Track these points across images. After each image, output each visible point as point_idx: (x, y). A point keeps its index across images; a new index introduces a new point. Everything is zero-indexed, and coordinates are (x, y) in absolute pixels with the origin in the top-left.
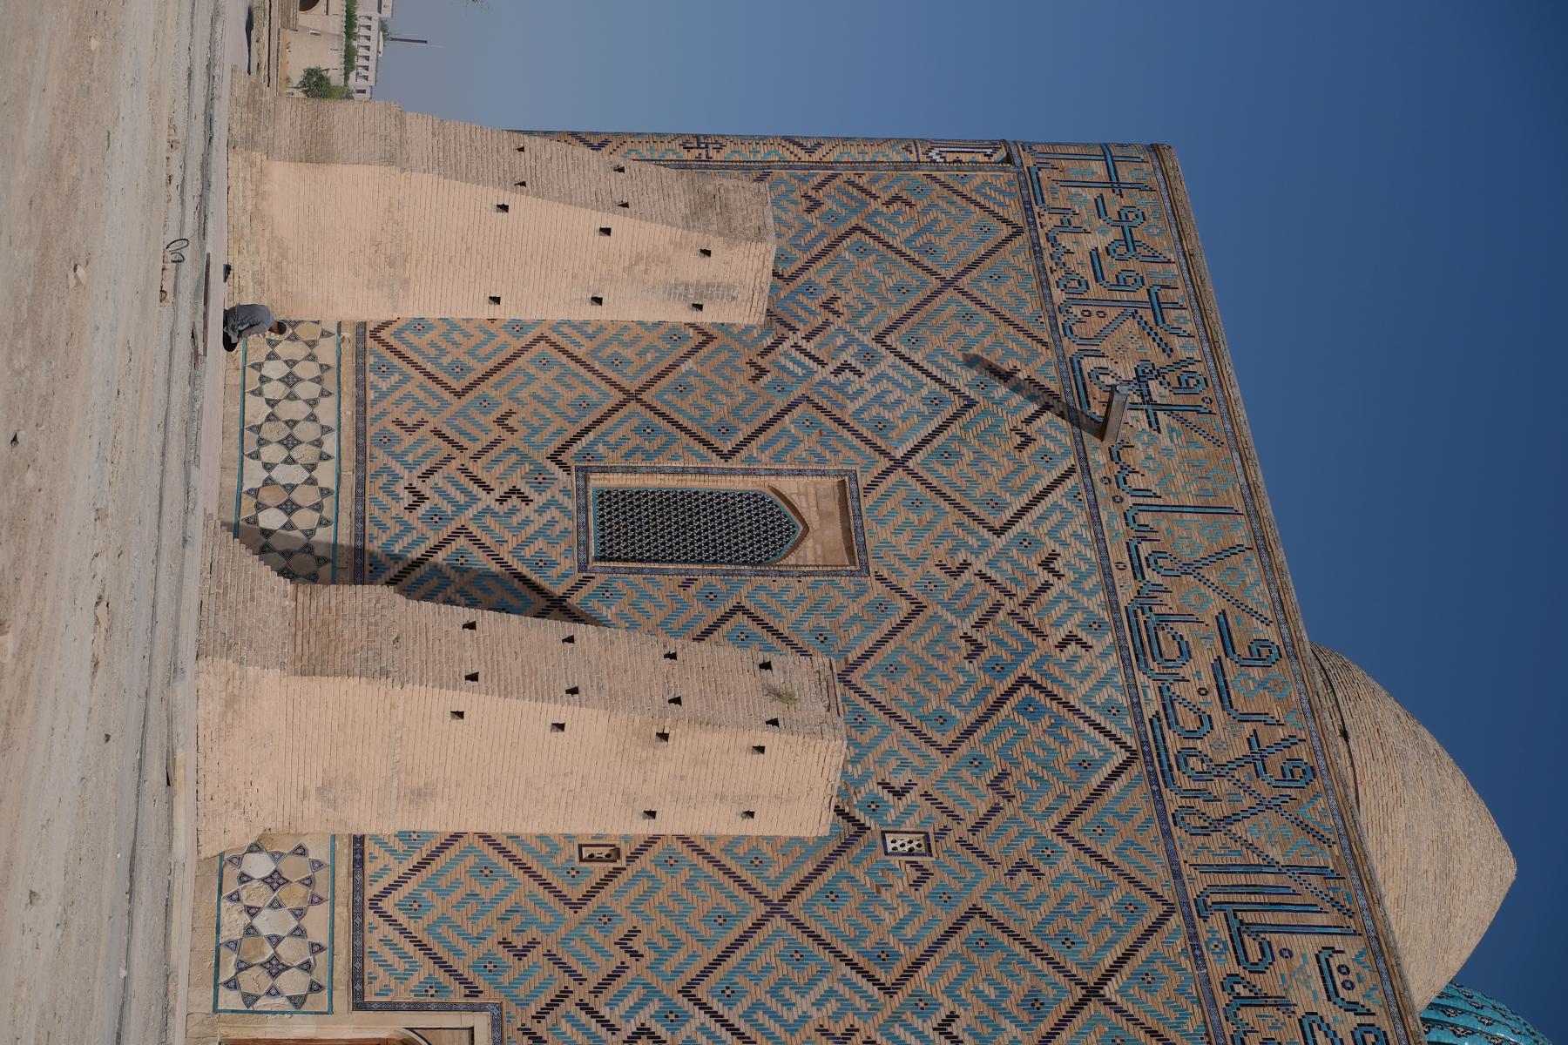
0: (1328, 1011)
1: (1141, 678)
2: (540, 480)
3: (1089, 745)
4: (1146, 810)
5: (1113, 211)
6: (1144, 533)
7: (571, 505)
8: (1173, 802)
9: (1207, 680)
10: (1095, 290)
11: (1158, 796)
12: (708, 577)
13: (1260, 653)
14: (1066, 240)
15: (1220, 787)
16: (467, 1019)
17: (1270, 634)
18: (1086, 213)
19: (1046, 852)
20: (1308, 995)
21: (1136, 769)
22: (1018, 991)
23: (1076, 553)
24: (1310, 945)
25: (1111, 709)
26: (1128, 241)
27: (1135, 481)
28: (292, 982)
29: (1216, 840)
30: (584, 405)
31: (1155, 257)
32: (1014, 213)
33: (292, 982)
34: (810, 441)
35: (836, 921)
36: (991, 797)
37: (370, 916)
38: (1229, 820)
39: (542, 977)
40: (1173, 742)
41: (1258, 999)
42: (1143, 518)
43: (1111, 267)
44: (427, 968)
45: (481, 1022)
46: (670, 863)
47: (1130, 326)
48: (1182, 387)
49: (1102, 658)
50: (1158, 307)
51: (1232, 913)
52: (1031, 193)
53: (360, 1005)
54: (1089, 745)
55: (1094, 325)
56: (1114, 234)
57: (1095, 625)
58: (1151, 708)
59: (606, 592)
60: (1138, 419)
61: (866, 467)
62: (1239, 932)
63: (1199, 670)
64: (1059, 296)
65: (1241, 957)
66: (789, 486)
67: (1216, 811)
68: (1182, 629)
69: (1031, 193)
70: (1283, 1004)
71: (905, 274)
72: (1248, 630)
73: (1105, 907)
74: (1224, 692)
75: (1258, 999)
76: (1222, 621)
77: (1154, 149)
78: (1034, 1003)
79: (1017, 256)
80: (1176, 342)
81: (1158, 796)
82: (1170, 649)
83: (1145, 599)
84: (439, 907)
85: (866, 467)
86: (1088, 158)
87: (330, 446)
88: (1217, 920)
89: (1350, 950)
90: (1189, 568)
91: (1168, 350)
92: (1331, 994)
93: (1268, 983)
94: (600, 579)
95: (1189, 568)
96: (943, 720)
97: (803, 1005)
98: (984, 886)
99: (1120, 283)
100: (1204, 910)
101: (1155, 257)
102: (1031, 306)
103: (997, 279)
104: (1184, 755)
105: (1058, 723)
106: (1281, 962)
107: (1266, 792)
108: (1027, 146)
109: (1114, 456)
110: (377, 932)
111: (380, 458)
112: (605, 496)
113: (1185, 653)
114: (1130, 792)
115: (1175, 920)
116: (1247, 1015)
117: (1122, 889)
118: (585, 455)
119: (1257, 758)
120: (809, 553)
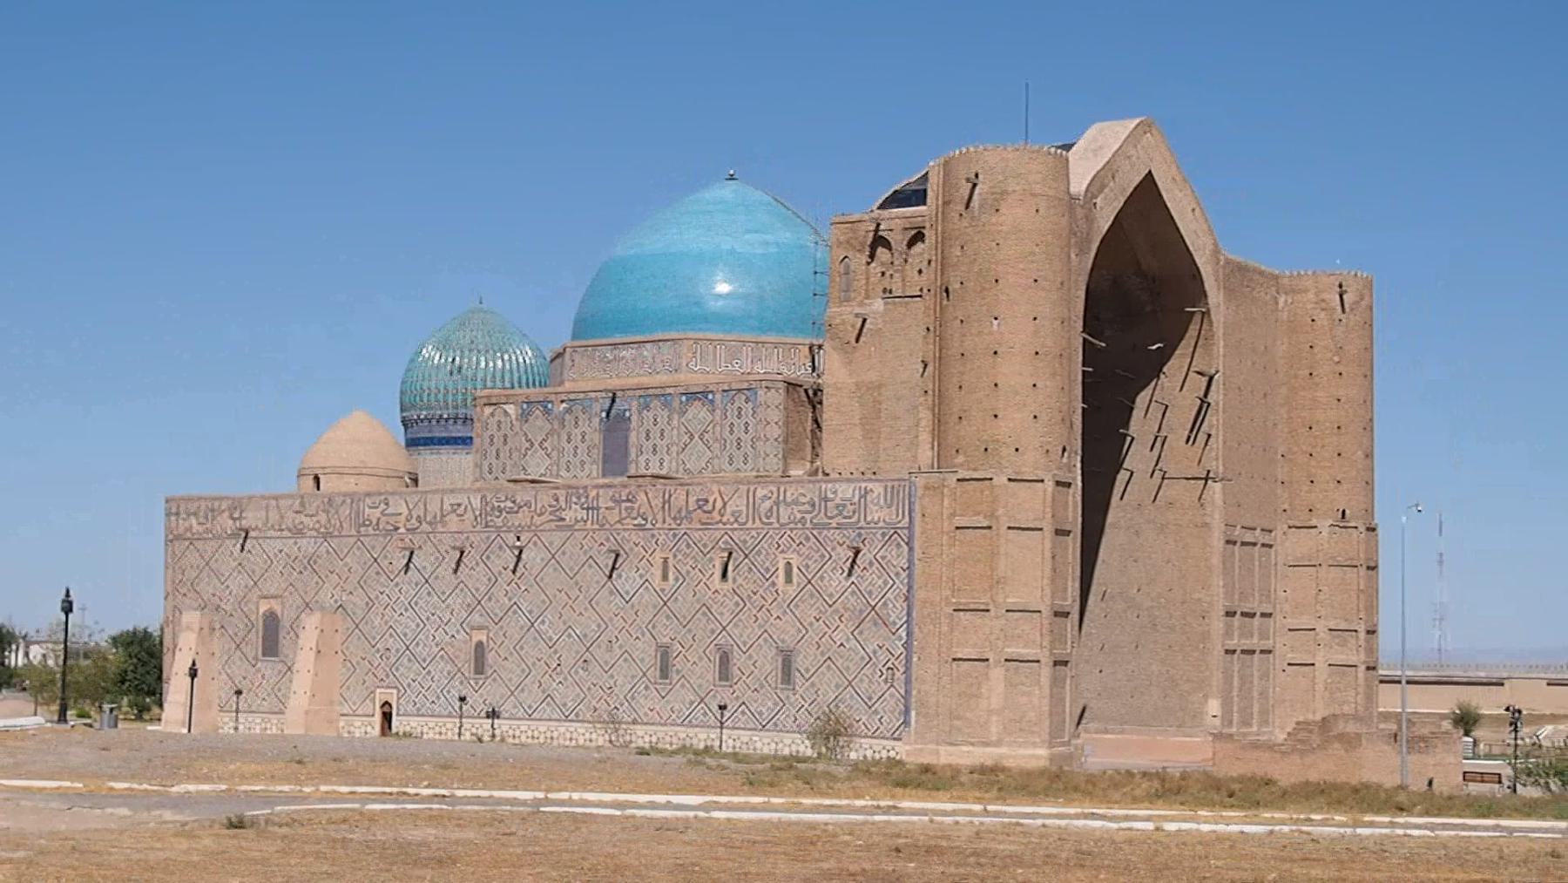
0: (380, 509)
1: (308, 535)
2: (259, 670)
3: (323, 549)
4: (336, 540)
5: (184, 516)
6: (273, 526)
7: (265, 664)
8: (336, 533)
9: (308, 518)
10: (209, 526)
11: (336, 536)
12: (282, 634)
13: (302, 504)
14: (194, 531)
15: (333, 522)
16: (377, 696)
17: (298, 502)
18: (187, 524)
19: (346, 564)
20: (377, 513)
21: (328, 539)
22: (375, 576)
23: (278, 544)
24: (367, 509)
25: (315, 543)
26: (195, 514)
27: (260, 526)
28: (369, 729)
29: (344, 525)
30: (241, 659)
31: (199, 508)
32: (187, 543)
33: (369, 729)
34: (250, 605)
35: (360, 613)
36: (334, 575)
37: (357, 713)
38: (341, 523)
39: (370, 679)
40: (322, 530)
41: (378, 524)
42: (269, 525)
43: (201, 520)
44: (367, 701)
45: (378, 690)
46: (347, 648)
47: (219, 518)
48: (235, 508)
49: (303, 542)
50: (213, 510)
51: (360, 526)
52: (178, 538)
53: (373, 715)
54: (323, 549)
55: (219, 528)
56: (192, 517)
57: (296, 543)
58: (315, 534)
59: (286, 656)
60: (244, 522)
61: (256, 593)
62: (365, 525)
63: (306, 520)
64: (210, 536)
65: (368, 526)
66: (261, 611)
67: (338, 524)
68: (297, 522)
69: (178, 538)
70: (379, 519)
71: (204, 574)
72: (297, 506)
73: (358, 553)
74: (312, 516)
75: (378, 524)
76: (297, 512)
77: (167, 501)
78: (378, 573)
79: (199, 544)
80: (223, 508)
81: (336, 536)
82: (301, 527)
83: (290, 530)
84: (355, 697)
85: (256, 593)
86: (169, 520)
87: (250, 719)
88: (362, 529)
89: (368, 501)
90: (282, 517)
91: (223, 511)
92: (377, 507)
93: (374, 522)
94: (282, 658)
95: (282, 517)
96: (317, 583)
97: (376, 623)
98: (354, 579)
99: (207, 518)
100: (359, 532)
101: (199, 508)
102: (212, 543)
103: (205, 551)
104: (326, 528)
105: (318, 556)
106: (371, 518)
107: (333, 511)
108: (167, 536)
109: (253, 530)
110: (360, 712)
111: (254, 708)
112: (264, 655)
113: (302, 523)
114: (334, 543)
115: (362, 539)
116: (381, 527)
117: (355, 549)
118: (253, 659)
119: (327, 512)
120: (278, 609)
